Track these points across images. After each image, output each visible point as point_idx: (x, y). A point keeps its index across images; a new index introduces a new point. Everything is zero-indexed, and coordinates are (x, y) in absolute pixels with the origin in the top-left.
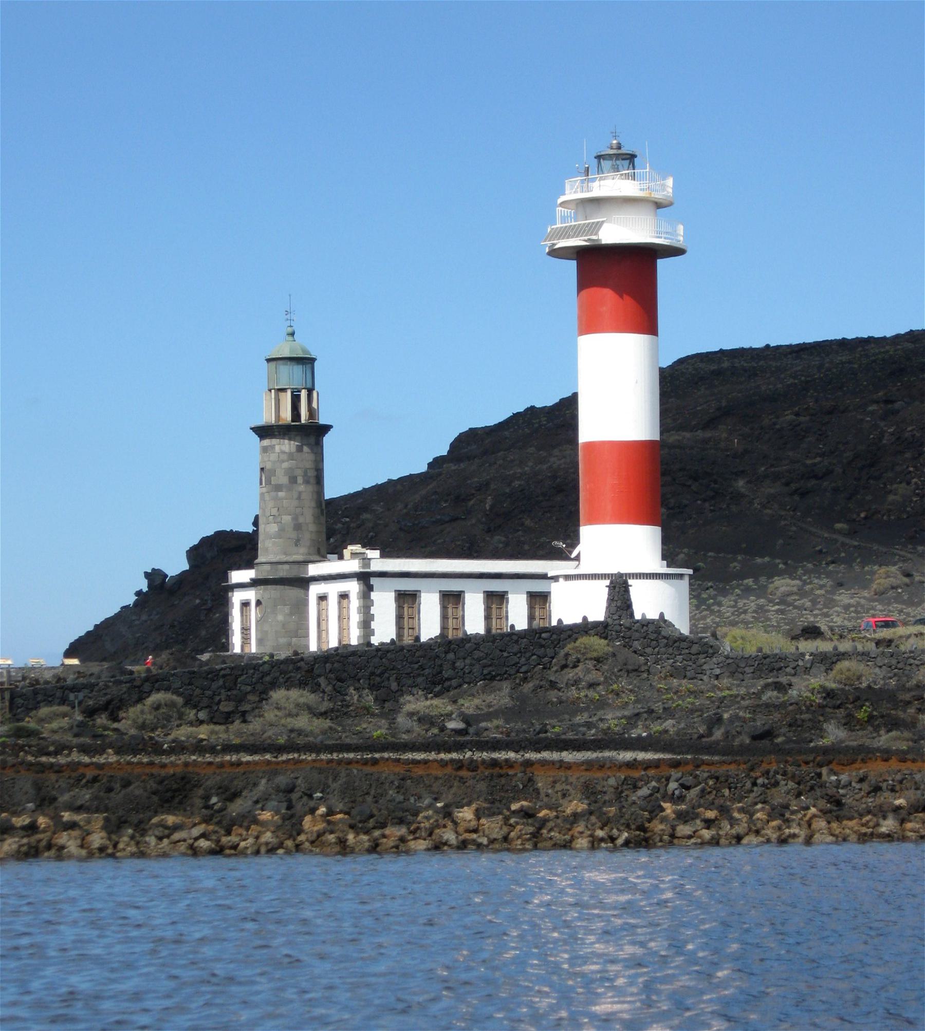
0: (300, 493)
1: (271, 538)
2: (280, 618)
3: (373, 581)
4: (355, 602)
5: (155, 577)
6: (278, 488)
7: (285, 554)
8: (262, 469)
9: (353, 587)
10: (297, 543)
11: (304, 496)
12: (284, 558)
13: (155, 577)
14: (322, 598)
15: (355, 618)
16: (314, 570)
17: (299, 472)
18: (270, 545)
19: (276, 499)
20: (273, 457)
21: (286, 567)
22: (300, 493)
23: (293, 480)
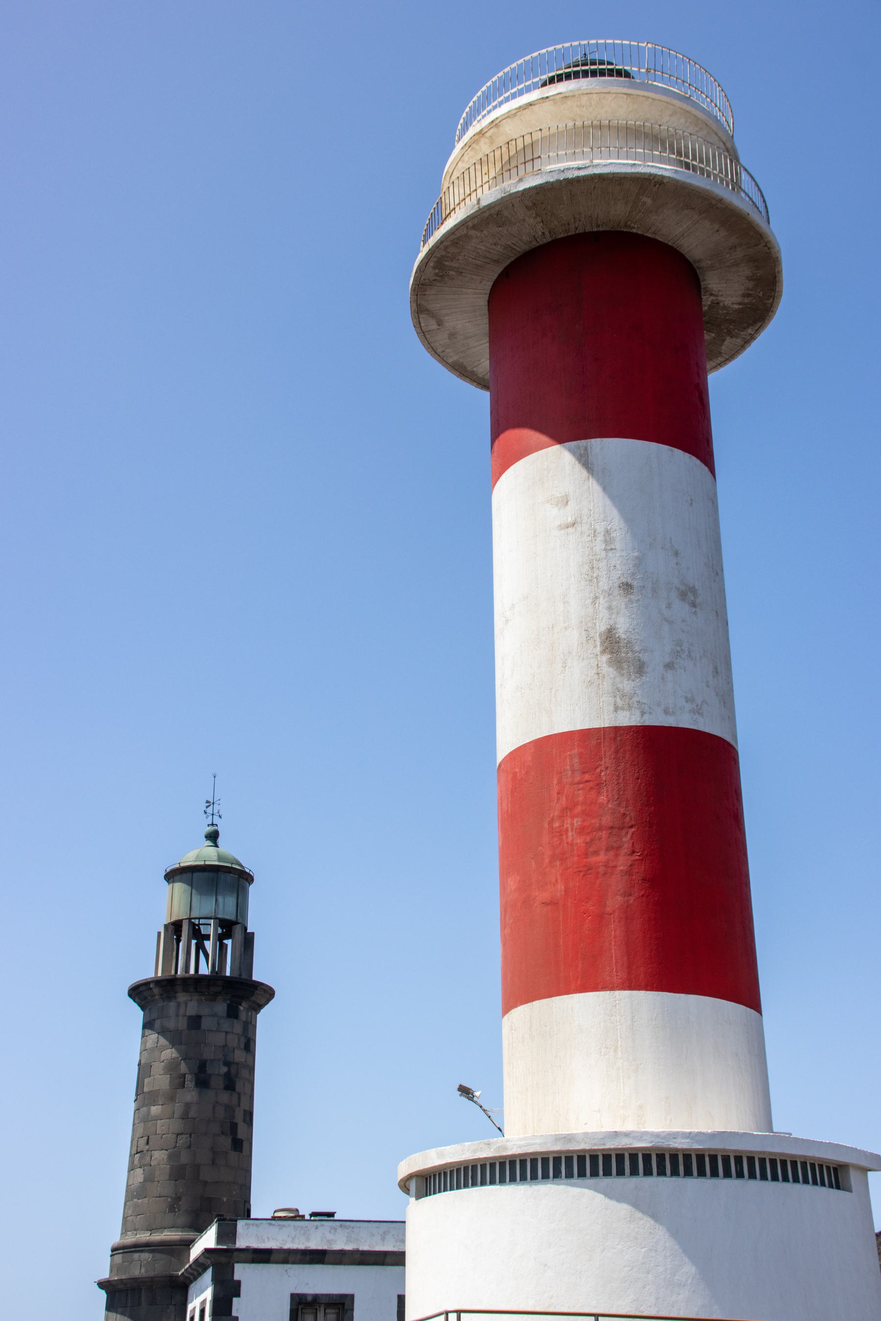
3: (241, 1272)
12: (144, 1237)
21: (146, 1256)
22: (188, 1106)
23: (180, 1083)
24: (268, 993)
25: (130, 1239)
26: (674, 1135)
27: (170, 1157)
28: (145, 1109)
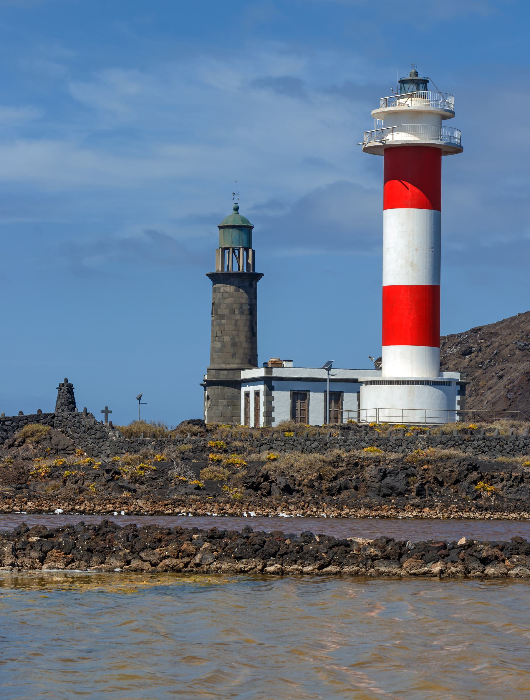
1: (216, 352)
2: (221, 408)
3: (274, 383)
4: (262, 398)
6: (222, 317)
8: (213, 303)
9: (262, 388)
10: (234, 356)
11: (239, 323)
12: (223, 366)
14: (247, 395)
15: (262, 409)
16: (245, 374)
17: (236, 306)
18: (216, 357)
19: (220, 325)
20: (219, 295)
21: (225, 372)
23: (232, 311)
26: (419, 378)
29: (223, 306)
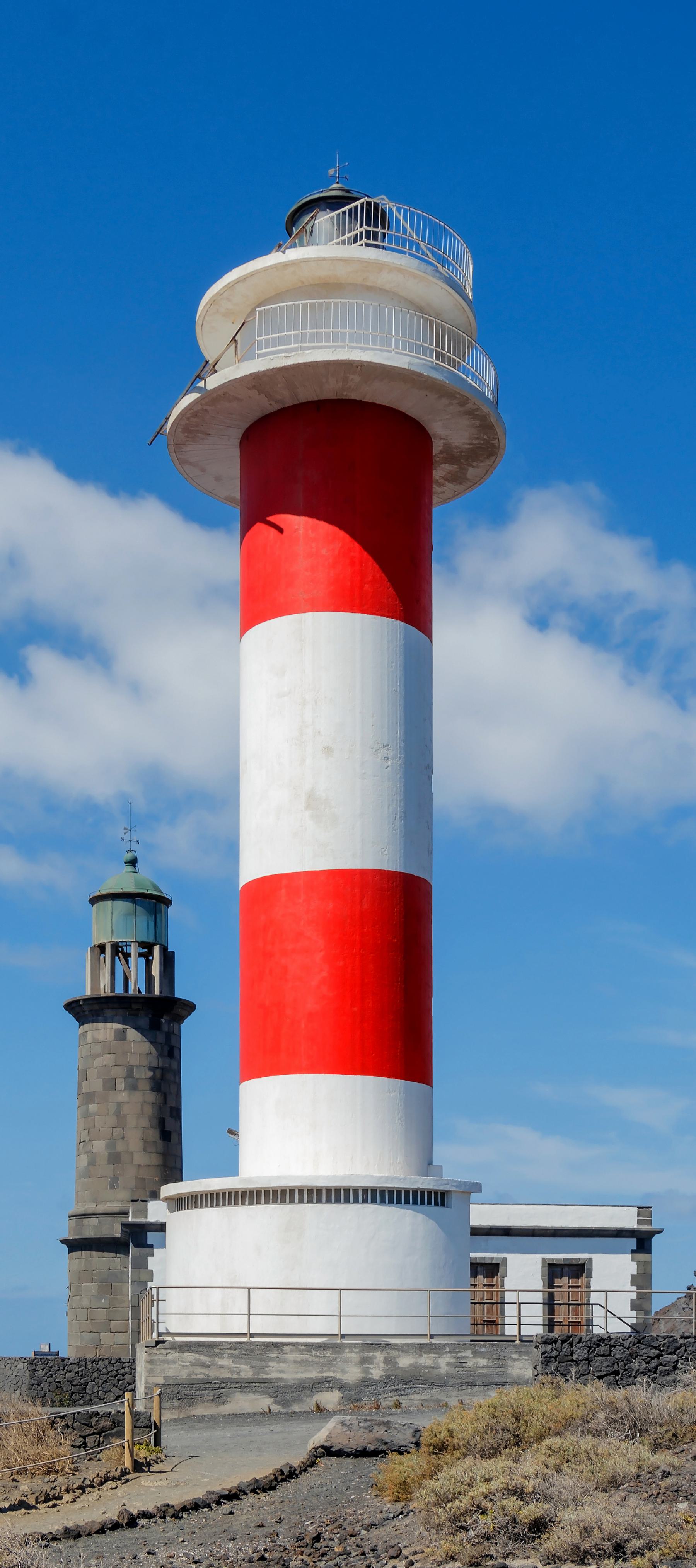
0: (119, 1105)
2: (86, 1302)
5: (632, 1276)
7: (97, 1201)
12: (91, 1207)
13: (632, 1276)
17: (119, 1073)
19: (86, 1115)
21: (94, 1221)
23: (110, 1084)
24: (190, 1007)
25: (80, 1209)
27: (107, 1146)
28: (84, 1107)
29: (92, 1074)
